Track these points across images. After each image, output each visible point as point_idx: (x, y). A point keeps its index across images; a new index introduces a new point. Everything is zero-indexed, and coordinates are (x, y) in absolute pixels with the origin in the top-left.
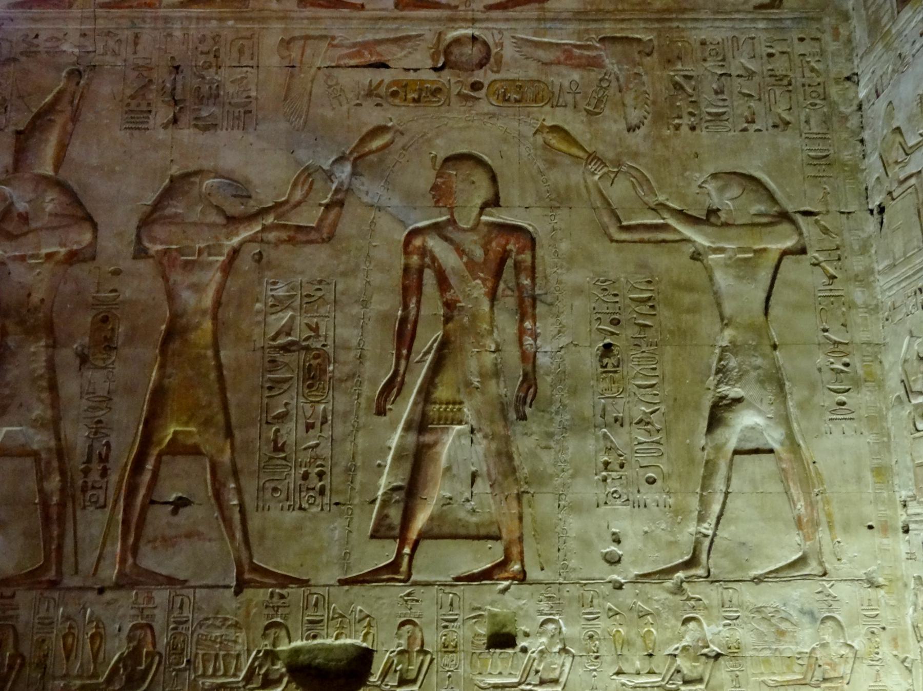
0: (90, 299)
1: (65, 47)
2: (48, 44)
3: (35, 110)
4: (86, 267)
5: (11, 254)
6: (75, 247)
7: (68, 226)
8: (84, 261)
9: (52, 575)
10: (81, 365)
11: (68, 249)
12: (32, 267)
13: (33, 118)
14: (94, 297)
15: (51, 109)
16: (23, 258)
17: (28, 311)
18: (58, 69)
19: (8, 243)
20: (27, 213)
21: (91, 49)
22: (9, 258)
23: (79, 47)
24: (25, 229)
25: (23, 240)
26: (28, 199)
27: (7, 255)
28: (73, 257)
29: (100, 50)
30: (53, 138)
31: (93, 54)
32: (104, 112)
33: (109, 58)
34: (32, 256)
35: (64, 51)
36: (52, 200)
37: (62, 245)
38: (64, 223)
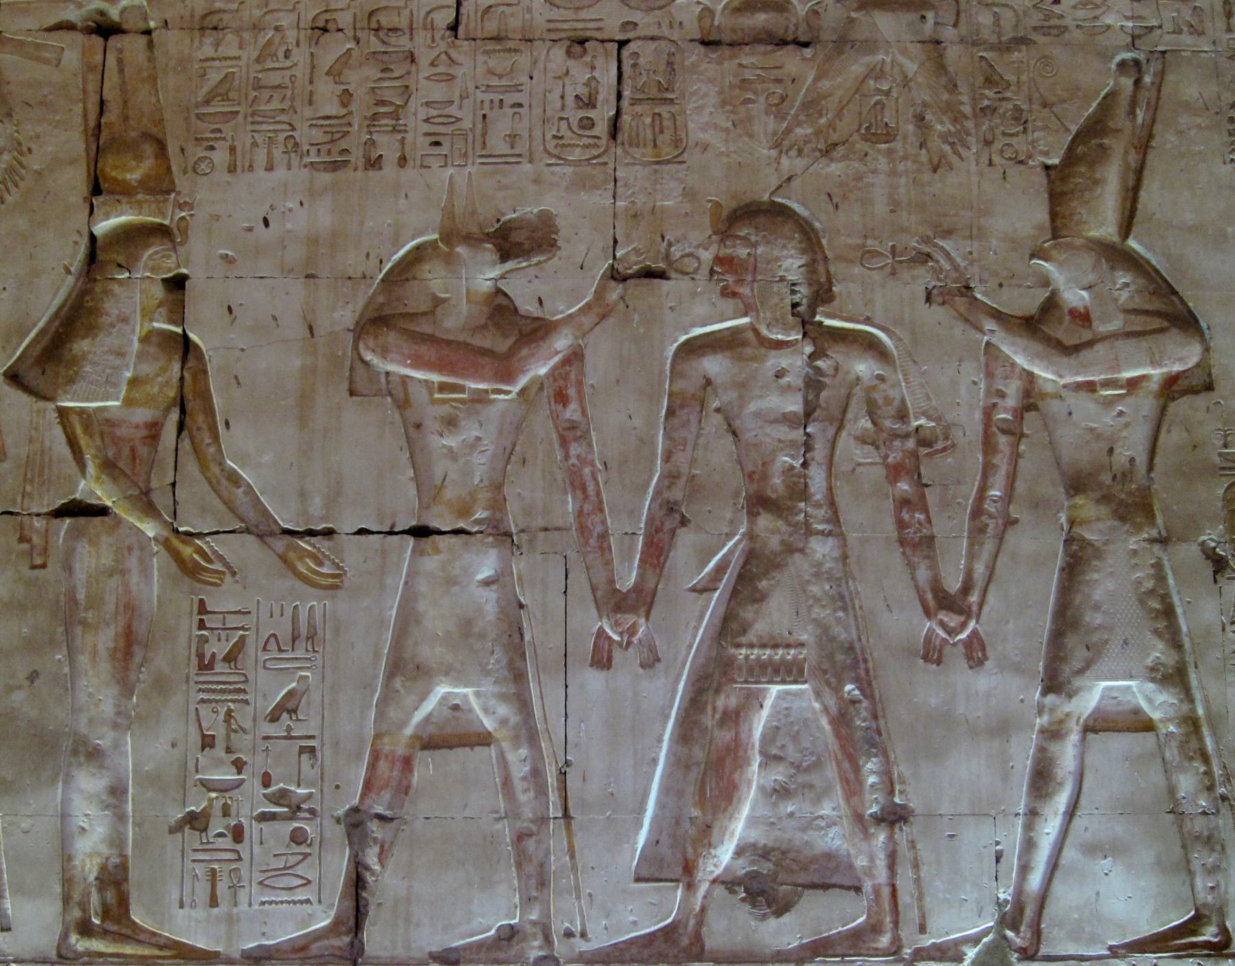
0: (1217, 460)
1: (1109, 20)
2: (1081, 14)
3: (1074, 129)
4: (1201, 401)
5: (1069, 379)
6: (1177, 368)
7: (1161, 331)
8: (1193, 391)
9: (1209, 934)
10: (1215, 573)
11: (1165, 370)
12: (1109, 403)
13: (1073, 141)
14: (1220, 455)
15: (1096, 128)
16: (1090, 387)
17: (1114, 477)
18: (1106, 56)
19: (1065, 360)
20: (1085, 307)
21: (1154, 23)
22: (1065, 386)
23: (1132, 18)
24: (1087, 335)
25: (1087, 355)
26: (1085, 283)
27: (1062, 382)
28: (1172, 388)
29: (1168, 26)
30: (1112, 177)
31: (1159, 32)
32: (1192, 133)
33: (1186, 39)
34: (1107, 384)
35: (1109, 27)
36: (1126, 285)
37: (1153, 363)
38: (1155, 326)
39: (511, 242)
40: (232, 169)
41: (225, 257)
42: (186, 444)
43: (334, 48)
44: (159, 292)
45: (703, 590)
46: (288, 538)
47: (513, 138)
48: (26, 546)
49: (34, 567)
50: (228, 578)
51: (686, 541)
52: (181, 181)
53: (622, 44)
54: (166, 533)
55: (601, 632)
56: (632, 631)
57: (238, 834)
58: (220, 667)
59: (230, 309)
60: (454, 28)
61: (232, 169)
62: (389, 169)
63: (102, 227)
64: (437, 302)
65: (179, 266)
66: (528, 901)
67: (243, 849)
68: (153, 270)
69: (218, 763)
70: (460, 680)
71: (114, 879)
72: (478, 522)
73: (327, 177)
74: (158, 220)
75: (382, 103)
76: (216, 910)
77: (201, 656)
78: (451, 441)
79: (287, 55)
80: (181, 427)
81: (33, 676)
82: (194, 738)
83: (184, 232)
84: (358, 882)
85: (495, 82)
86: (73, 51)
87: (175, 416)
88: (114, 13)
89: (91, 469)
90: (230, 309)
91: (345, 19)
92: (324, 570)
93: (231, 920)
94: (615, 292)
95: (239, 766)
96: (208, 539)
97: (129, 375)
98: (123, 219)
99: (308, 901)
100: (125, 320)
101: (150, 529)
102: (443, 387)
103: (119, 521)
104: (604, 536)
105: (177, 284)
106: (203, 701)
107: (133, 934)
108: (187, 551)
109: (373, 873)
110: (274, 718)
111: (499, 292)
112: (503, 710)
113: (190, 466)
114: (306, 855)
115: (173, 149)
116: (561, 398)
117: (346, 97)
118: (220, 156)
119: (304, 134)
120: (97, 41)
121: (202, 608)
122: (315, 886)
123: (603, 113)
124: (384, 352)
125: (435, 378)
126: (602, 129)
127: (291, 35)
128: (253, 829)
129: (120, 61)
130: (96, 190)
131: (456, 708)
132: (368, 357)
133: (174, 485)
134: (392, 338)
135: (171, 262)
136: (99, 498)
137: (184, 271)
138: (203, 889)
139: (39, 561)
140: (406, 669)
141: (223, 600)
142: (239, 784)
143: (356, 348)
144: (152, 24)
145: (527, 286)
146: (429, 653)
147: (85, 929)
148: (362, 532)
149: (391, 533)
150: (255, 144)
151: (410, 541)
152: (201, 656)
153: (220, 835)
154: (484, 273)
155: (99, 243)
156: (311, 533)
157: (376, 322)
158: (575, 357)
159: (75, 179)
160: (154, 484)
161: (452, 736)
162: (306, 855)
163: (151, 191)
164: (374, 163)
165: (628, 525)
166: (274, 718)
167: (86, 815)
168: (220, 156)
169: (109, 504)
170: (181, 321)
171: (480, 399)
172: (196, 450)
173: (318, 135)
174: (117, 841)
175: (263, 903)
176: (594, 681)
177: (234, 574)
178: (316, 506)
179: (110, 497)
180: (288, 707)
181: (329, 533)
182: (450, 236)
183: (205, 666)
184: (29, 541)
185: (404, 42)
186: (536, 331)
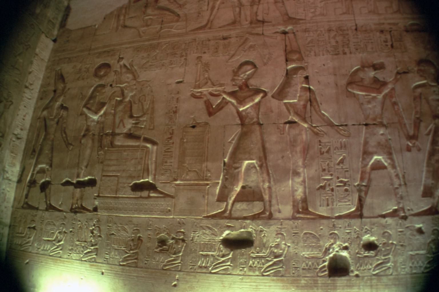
39: (375, 67)
40: (315, 55)
41: (316, 72)
42: (312, 108)
43: (333, 34)
44: (303, 79)
45: (428, 134)
46: (337, 127)
47: (372, 48)
48: (279, 130)
49: (281, 134)
50: (325, 135)
51: (422, 125)
52: (305, 58)
53: (390, 31)
54: (309, 126)
55: (408, 145)
56: (414, 144)
57: (332, 190)
58: (325, 154)
59: (319, 82)
60: (356, 29)
61: (315, 55)
62: (348, 55)
63: (289, 67)
64: (362, 79)
65: (306, 74)
66: (399, 203)
67: (334, 193)
68: (301, 75)
69: (326, 175)
70: (379, 155)
71: (305, 200)
72: (378, 122)
73: (335, 56)
74: (301, 65)
75: (344, 43)
76: (328, 207)
77: (321, 151)
78: (370, 106)
79: (323, 35)
80: (311, 105)
81: (283, 157)
82: (321, 169)
83: (307, 68)
84: (360, 200)
85: (366, 38)
86: (279, 37)
87: (309, 103)
88: (287, 30)
89: (292, 114)
90: (319, 82)
91: (334, 29)
92: (346, 133)
93: (332, 209)
94: (399, 77)
95: (331, 175)
96: (320, 127)
97: (298, 95)
98: (294, 66)
99: (349, 205)
100: (297, 84)
101: (306, 125)
102: (366, 95)
103: (299, 125)
104: (405, 124)
105: (307, 78)
106: (322, 161)
107: (310, 213)
108: (315, 130)
109: (363, 198)
110: (338, 164)
111: (375, 77)
112: (389, 161)
113: (314, 112)
114: (348, 194)
115: (302, 52)
116: (391, 97)
117: (337, 42)
118: (313, 53)
119: (329, 49)
120: (284, 35)
121: (320, 141)
122: (351, 201)
123: (389, 43)
124: (353, 89)
125: (364, 93)
126: (390, 46)
127: (324, 32)
128: (336, 189)
129: (289, 39)
130: (287, 61)
131: (378, 161)
132: (350, 90)
133: (311, 117)
134: (354, 86)
135: (305, 73)
136: (294, 120)
137: (308, 75)
138: (325, 203)
139: (282, 133)
140: (367, 154)
141: (325, 140)
142: (331, 179)
143: (346, 88)
144: (294, 31)
145: (380, 75)
146: (371, 149)
147: (299, 212)
148: (354, 125)
149: (360, 125)
150: (319, 51)
151: (364, 127)
152: (321, 151)
153: (328, 190)
154: (372, 74)
155: (288, 71)
156: (342, 125)
157: (350, 83)
158: (393, 89)
159: (283, 58)
160: (306, 116)
161: (378, 166)
162: (348, 194)
163: (298, 60)
164: (345, 53)
165: (409, 122)
166: (338, 164)
167: (297, 187)
168: (313, 53)
169: (297, 120)
170: (308, 84)
171: (374, 98)
172: (315, 109)
173: (332, 49)
174: (305, 193)
175: (339, 205)
176: (408, 154)
177: (326, 134)
178: (343, 119)
179: (297, 119)
180: (342, 162)
181: (346, 125)
182: (363, 67)
183: (322, 153)
184: (279, 129)
185: (346, 32)
186: (384, 84)
